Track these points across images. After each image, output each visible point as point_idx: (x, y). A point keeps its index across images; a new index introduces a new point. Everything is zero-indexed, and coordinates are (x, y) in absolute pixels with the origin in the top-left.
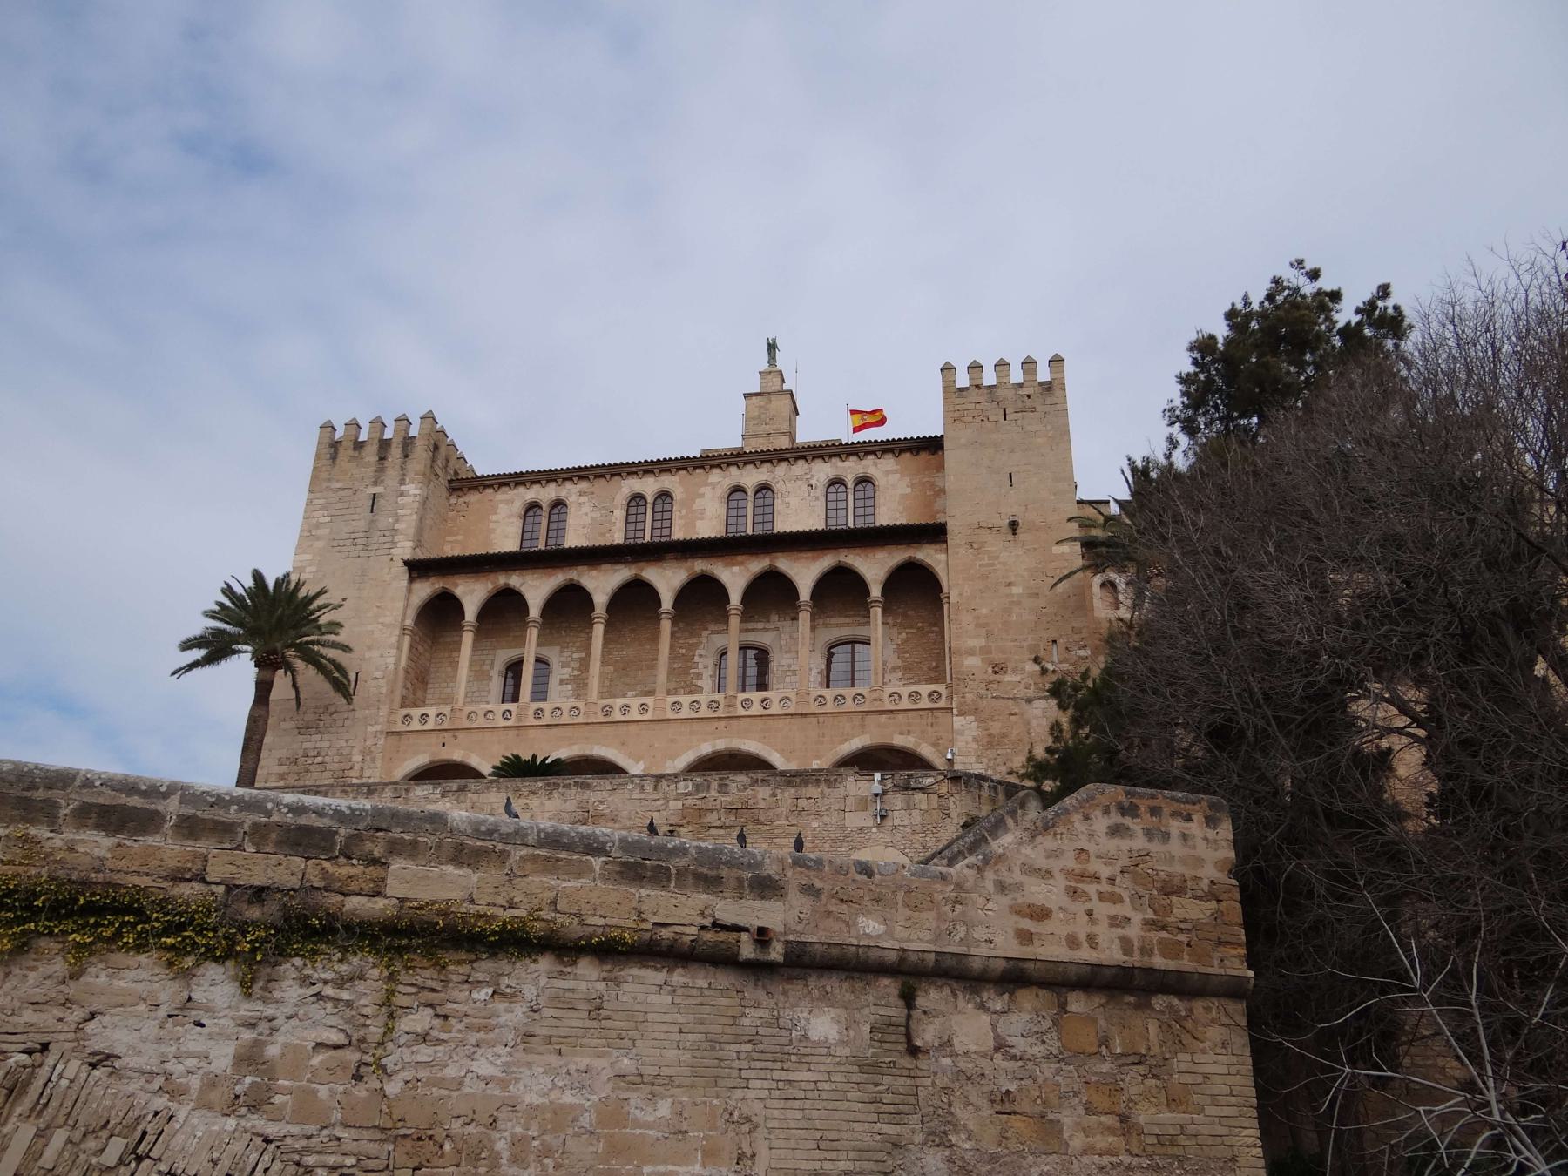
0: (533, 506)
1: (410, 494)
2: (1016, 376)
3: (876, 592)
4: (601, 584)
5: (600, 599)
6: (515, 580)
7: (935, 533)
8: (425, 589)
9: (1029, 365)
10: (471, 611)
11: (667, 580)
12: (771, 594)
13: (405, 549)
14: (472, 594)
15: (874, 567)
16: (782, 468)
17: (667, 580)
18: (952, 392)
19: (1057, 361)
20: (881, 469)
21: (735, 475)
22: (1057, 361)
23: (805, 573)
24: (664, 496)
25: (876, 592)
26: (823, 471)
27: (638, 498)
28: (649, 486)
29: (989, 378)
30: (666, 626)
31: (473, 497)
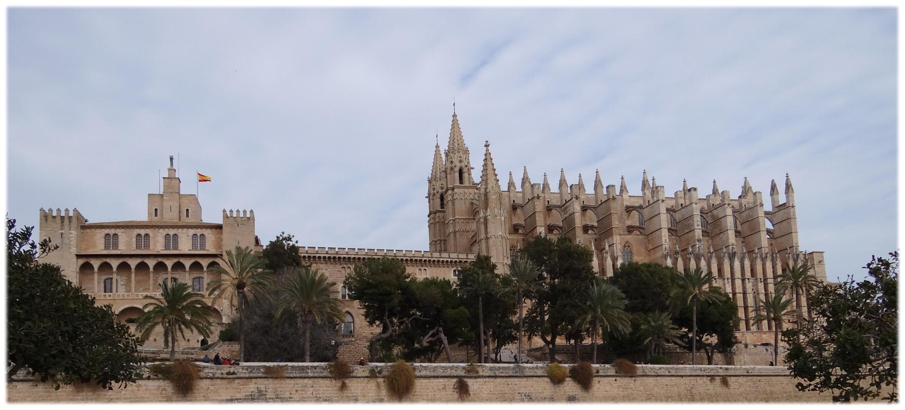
0: (107, 235)
1: (73, 234)
2: (242, 215)
3: (205, 269)
4: (133, 263)
5: (133, 267)
6: (108, 260)
7: (220, 256)
8: (81, 261)
9: (245, 212)
10: (96, 269)
11: (151, 263)
12: (178, 266)
13: (74, 251)
14: (96, 264)
15: (205, 263)
16: (180, 230)
17: (151, 263)
18: (226, 217)
19: (251, 211)
20: (207, 232)
21: (167, 231)
22: (251, 211)
23: (187, 263)
24: (147, 235)
25: (205, 269)
26: (191, 232)
27: (139, 235)
28: (143, 232)
29: (235, 215)
30: (151, 275)
31: (88, 231)
